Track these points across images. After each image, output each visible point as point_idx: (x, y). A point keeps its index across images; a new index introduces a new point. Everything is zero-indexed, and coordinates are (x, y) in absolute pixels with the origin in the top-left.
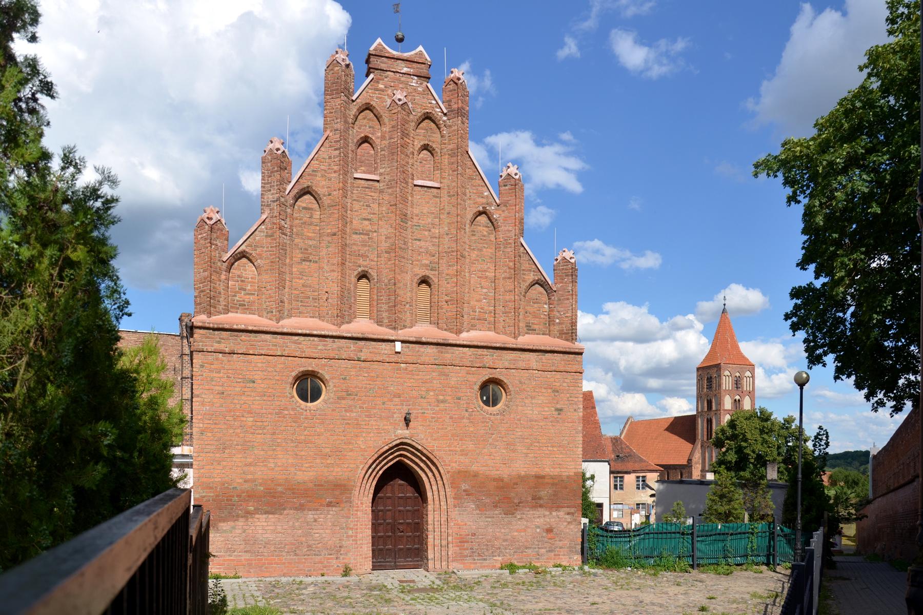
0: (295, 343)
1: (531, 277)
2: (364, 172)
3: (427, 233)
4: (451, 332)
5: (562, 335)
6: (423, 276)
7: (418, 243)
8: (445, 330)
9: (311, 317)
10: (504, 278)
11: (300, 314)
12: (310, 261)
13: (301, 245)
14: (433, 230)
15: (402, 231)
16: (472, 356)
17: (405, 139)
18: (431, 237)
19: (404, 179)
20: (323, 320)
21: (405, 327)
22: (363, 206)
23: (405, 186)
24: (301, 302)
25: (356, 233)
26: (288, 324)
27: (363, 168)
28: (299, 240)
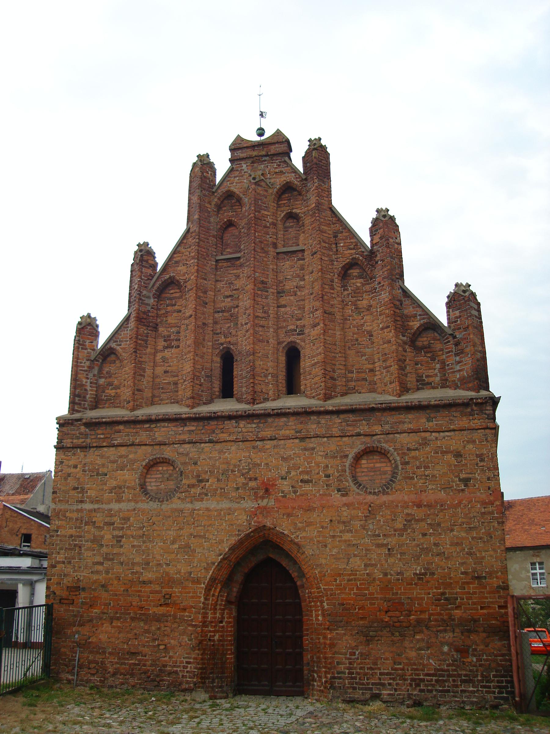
0: (146, 430)
1: (416, 324)
2: (231, 253)
3: (292, 298)
4: (318, 399)
5: (463, 384)
6: (288, 343)
7: (283, 309)
8: (314, 397)
9: (171, 403)
10: (382, 329)
11: (161, 402)
12: (173, 347)
13: (166, 333)
14: (299, 293)
15: (260, 299)
16: (343, 424)
17: (263, 212)
18: (297, 301)
19: (262, 249)
20: (180, 405)
21: (266, 400)
22: (226, 284)
23: (264, 255)
24: (162, 388)
25: (219, 312)
26: (141, 413)
27: (228, 250)
28: (163, 329)
